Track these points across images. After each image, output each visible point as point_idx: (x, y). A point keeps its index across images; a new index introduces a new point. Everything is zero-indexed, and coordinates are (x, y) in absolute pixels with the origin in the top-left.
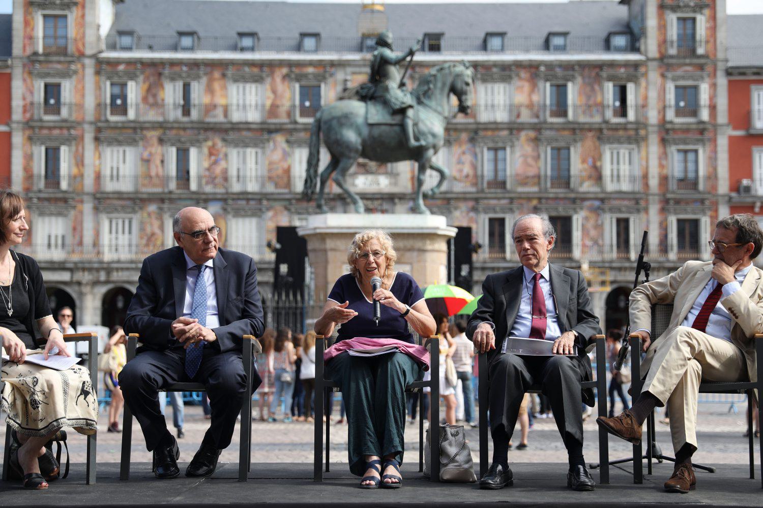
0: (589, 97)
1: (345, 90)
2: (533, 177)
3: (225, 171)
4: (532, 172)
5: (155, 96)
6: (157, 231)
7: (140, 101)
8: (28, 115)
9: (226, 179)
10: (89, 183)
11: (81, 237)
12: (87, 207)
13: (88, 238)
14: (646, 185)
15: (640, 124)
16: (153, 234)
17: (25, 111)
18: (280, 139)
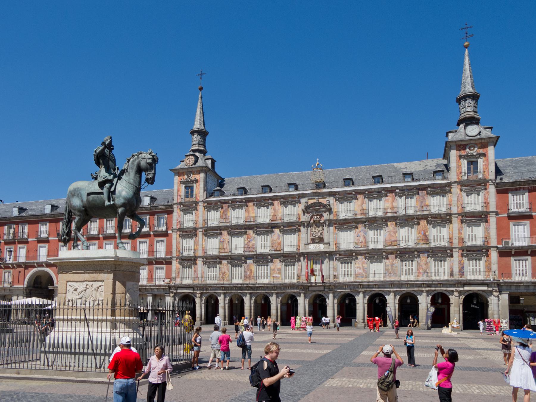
2: (394, 241)
4: (393, 239)
5: (226, 215)
8: (179, 226)
10: (200, 253)
18: (277, 231)
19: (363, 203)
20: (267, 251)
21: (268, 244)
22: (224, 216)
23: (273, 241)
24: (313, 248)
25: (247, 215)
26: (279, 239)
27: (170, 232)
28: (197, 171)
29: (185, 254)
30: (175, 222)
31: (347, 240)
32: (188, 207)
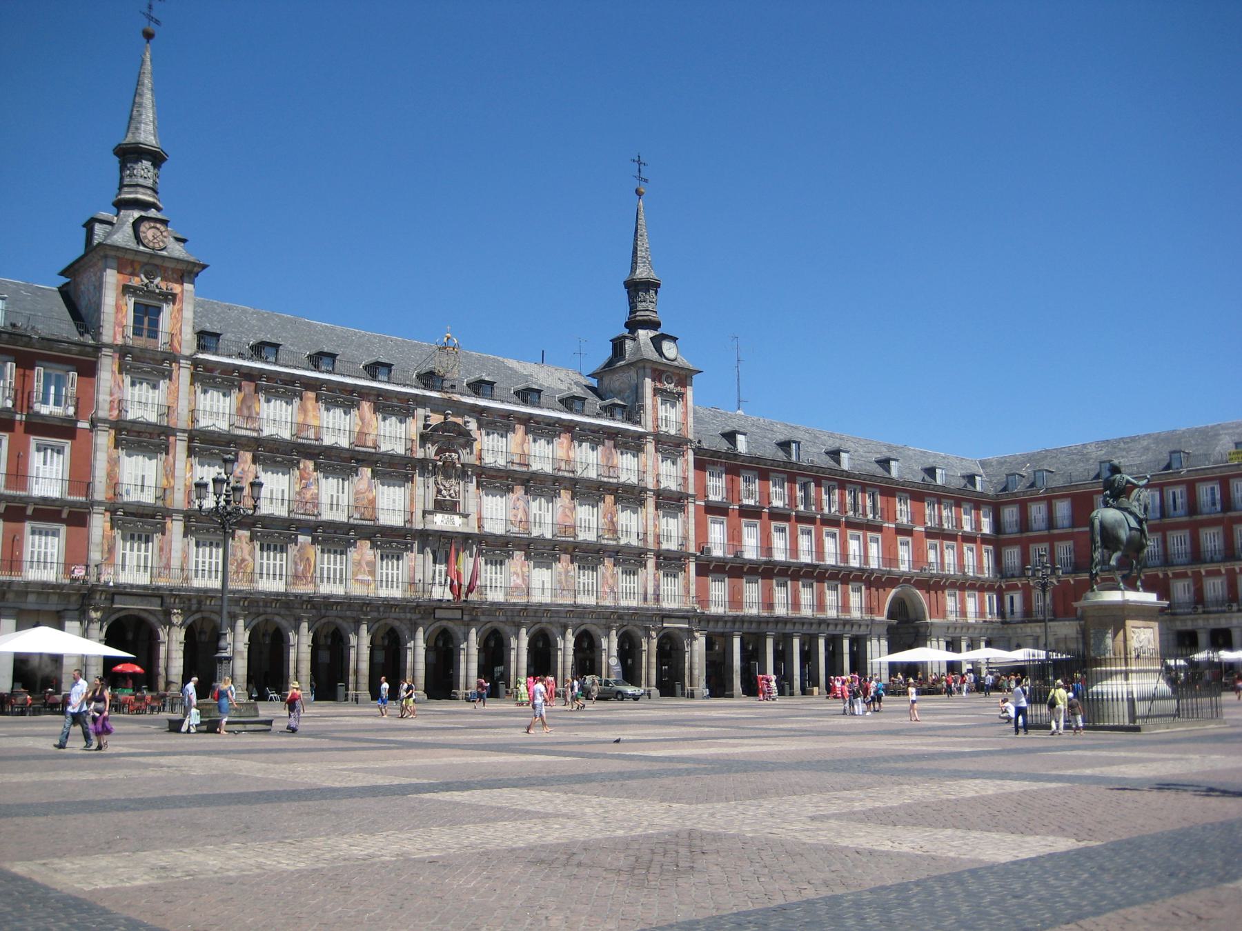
0: (608, 459)
1: (426, 427)
2: (570, 527)
3: (316, 497)
5: (249, 408)
6: (247, 557)
7: (233, 411)
9: (316, 505)
11: (169, 559)
12: (176, 527)
13: (176, 563)
14: (645, 540)
15: (645, 490)
16: (243, 560)
17: (111, 409)
18: (367, 472)
19: (523, 442)
20: (341, 516)
21: (344, 500)
22: (246, 412)
23: (357, 493)
24: (440, 522)
25: (300, 420)
26: (371, 491)
27: (83, 424)
28: (174, 270)
29: (133, 496)
30: (104, 398)
31: (495, 513)
32: (147, 364)
